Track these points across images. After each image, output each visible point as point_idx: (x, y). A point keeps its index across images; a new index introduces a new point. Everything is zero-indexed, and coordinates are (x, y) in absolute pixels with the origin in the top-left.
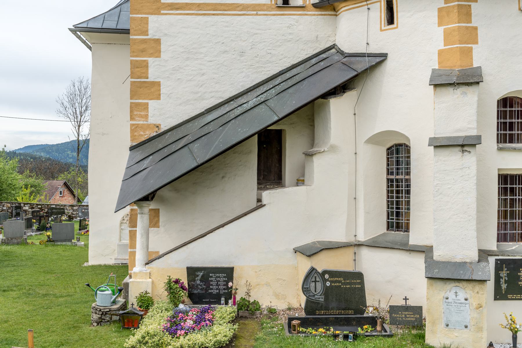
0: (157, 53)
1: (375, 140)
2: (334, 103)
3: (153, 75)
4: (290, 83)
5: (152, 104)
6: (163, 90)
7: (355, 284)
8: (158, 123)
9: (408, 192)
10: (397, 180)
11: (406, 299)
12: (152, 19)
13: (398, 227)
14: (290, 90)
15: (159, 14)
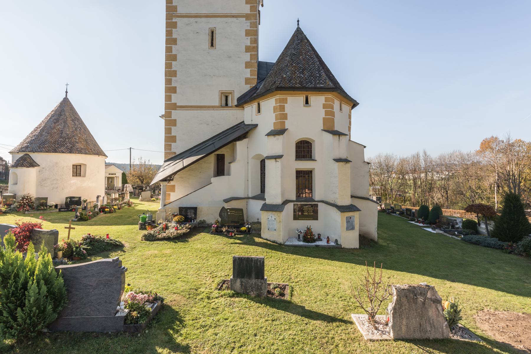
7: (240, 213)
8: (175, 151)
11: (258, 219)
15: (176, 110)
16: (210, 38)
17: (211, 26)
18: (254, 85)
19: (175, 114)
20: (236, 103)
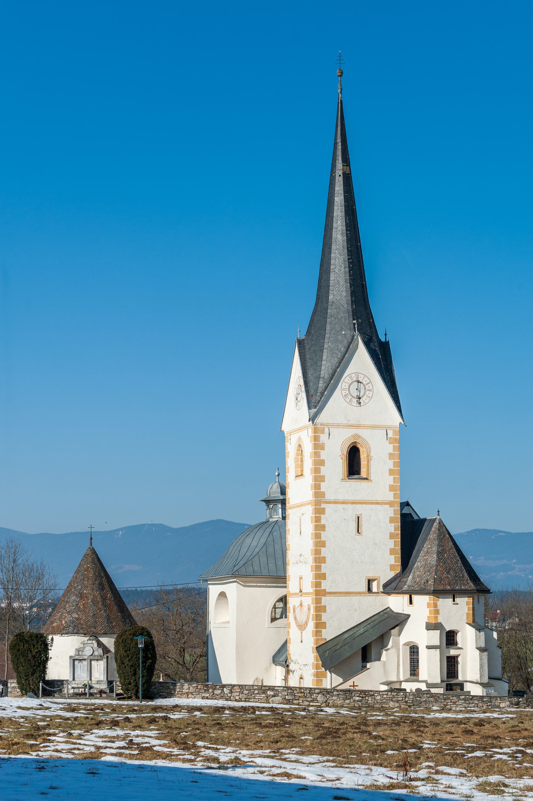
0: (325, 611)
1: (406, 644)
2: (392, 631)
3: (324, 619)
4: (375, 623)
5: (323, 631)
6: (327, 625)
9: (418, 662)
10: (414, 658)
12: (323, 598)
14: (377, 626)
16: (357, 525)
17: (358, 513)
18: (398, 572)
19: (325, 600)
20: (382, 590)
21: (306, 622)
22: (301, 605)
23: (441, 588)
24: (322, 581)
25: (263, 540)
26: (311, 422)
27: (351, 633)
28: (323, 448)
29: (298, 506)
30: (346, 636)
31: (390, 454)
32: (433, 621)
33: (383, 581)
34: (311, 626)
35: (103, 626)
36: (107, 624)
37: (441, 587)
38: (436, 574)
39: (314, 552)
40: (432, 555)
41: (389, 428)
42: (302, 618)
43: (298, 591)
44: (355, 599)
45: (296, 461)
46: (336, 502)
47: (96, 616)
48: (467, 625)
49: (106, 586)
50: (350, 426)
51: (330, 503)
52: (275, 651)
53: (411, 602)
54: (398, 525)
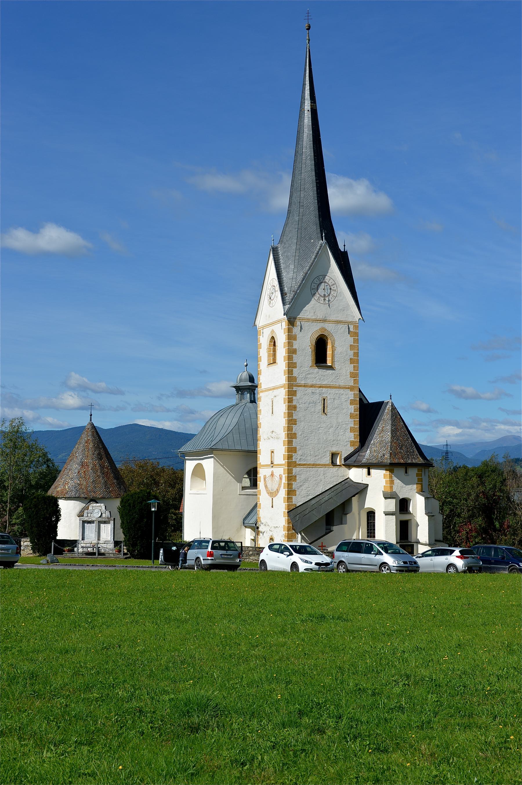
2: (353, 498)
3: (294, 487)
5: (294, 497)
12: (294, 469)
13: (371, 537)
19: (295, 470)
20: (343, 462)
21: (277, 490)
22: (272, 475)
23: (396, 461)
24: (294, 454)
25: (235, 420)
26: (285, 316)
27: (317, 499)
28: (295, 339)
29: (271, 390)
30: (313, 502)
31: (351, 345)
32: (389, 490)
33: (345, 455)
34: (283, 493)
35: (101, 491)
36: (105, 490)
37: (396, 461)
38: (391, 450)
39: (286, 429)
40: (387, 432)
41: (350, 323)
42: (273, 485)
43: (270, 463)
44: (321, 470)
45: (269, 351)
46: (305, 386)
47: (95, 482)
48: (417, 494)
49: (104, 456)
50: (318, 320)
51: (300, 386)
52: (245, 514)
53: (369, 474)
54: (357, 407)
